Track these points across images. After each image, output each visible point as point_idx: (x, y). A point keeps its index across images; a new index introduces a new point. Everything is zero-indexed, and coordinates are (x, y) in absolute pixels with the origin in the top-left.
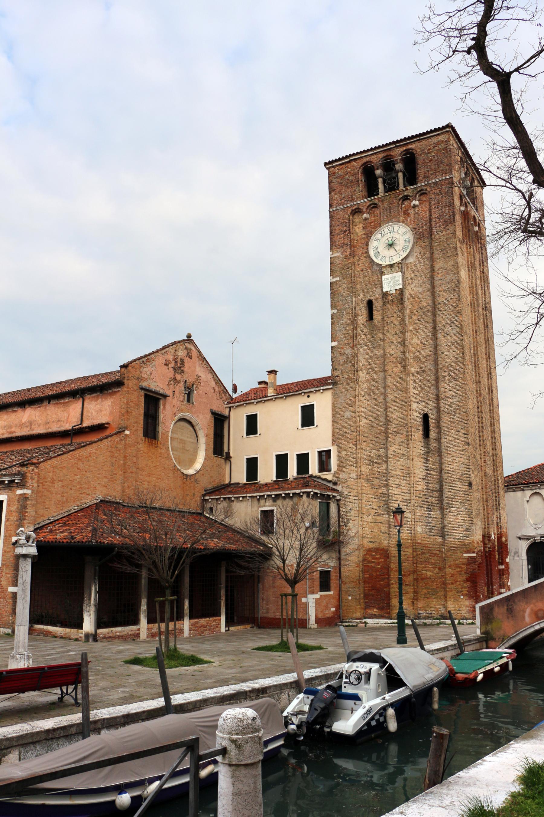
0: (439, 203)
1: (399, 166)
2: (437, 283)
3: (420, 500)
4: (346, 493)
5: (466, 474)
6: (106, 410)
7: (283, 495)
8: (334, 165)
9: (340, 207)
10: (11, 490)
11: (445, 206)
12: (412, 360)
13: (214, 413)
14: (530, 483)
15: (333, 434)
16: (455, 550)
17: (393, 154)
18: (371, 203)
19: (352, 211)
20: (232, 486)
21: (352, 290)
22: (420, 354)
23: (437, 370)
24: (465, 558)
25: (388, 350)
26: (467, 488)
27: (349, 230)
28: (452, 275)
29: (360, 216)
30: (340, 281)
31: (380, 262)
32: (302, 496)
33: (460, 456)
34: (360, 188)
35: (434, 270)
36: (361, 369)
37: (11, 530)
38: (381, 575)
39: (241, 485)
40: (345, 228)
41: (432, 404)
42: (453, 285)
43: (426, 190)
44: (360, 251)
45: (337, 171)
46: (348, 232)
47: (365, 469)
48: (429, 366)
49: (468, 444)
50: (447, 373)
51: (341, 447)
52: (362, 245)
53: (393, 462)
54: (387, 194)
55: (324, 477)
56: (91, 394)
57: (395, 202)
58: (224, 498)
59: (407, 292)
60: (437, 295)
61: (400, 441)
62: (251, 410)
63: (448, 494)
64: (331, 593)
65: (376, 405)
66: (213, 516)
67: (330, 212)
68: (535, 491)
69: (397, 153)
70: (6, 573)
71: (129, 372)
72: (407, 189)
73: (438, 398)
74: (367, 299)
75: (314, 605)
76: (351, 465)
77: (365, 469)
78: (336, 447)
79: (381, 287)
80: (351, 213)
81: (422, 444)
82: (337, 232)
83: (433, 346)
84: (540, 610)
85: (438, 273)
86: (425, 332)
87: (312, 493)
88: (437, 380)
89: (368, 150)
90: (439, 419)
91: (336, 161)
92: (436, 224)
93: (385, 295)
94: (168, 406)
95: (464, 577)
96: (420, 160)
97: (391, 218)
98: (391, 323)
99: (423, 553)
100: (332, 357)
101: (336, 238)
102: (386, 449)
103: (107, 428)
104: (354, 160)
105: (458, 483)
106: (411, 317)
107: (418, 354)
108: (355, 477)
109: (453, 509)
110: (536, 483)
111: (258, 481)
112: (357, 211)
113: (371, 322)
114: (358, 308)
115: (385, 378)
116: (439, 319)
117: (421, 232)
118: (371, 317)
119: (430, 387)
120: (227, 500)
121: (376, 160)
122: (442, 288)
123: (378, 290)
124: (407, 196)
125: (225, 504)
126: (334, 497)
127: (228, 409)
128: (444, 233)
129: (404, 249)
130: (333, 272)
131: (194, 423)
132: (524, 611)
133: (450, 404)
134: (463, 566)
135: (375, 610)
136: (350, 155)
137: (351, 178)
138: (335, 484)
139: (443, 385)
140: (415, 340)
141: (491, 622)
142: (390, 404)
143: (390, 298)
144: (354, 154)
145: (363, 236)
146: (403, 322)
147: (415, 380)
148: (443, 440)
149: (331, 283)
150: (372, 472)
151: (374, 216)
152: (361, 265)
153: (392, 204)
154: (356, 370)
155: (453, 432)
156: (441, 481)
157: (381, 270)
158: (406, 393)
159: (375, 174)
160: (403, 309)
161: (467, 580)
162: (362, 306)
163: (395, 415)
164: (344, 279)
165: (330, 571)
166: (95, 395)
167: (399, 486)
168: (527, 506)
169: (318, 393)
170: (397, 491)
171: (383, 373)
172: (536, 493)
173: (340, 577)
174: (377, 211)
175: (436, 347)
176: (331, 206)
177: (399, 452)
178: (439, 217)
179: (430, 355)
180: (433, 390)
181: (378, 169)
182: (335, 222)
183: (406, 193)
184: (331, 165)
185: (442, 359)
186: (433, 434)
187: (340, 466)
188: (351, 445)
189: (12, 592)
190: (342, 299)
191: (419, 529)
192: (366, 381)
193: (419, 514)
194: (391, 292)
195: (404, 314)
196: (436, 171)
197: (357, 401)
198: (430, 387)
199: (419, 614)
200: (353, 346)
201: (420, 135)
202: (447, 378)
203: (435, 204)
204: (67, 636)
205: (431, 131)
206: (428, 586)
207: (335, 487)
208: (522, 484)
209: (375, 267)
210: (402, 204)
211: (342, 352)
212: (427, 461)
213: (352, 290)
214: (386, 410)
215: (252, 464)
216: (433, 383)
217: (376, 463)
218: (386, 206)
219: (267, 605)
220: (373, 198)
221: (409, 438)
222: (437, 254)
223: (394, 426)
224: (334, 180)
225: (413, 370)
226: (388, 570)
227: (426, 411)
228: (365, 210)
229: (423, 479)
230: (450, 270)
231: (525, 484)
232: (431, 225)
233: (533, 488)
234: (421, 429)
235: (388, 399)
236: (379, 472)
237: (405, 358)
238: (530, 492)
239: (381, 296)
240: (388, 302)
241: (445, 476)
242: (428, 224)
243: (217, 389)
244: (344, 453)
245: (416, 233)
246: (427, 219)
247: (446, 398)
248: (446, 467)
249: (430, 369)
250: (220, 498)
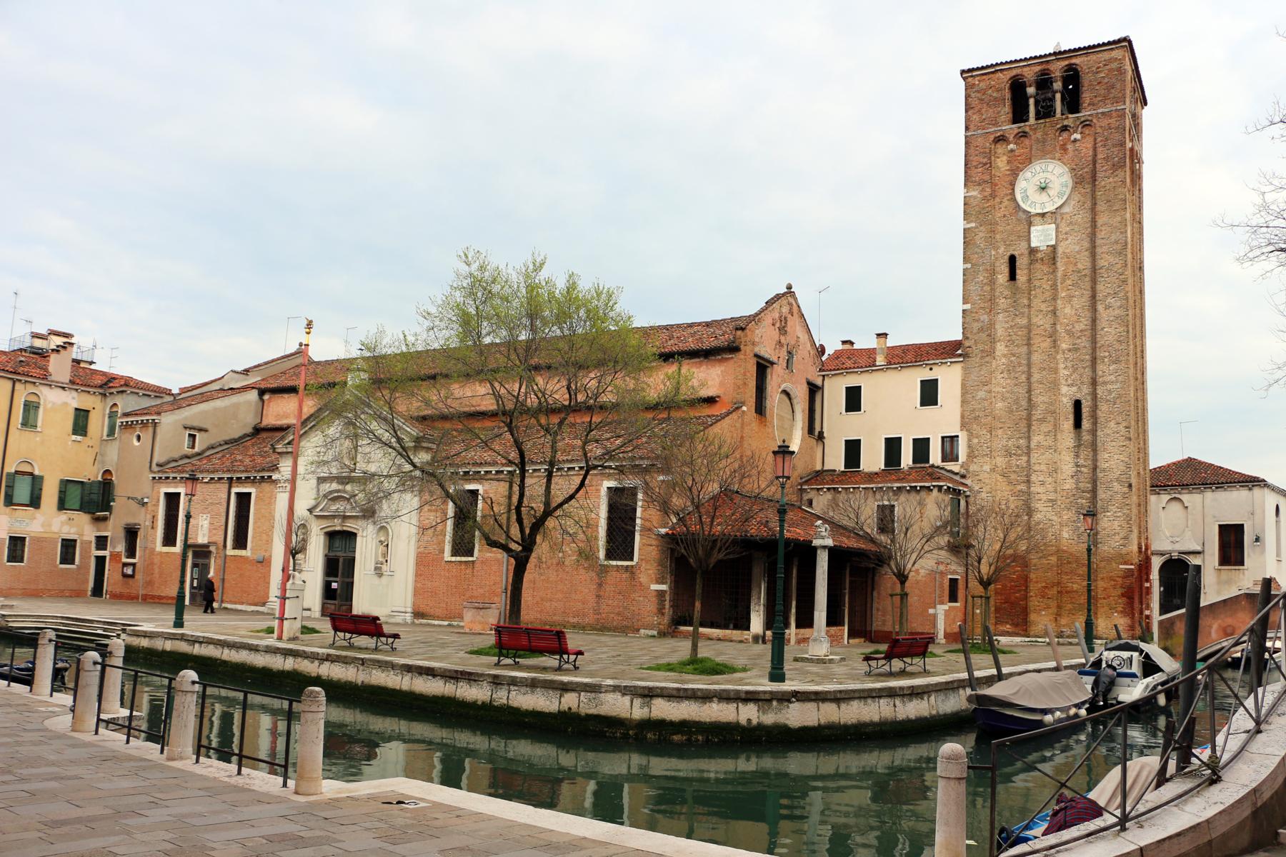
0: (1107, 140)
1: (1058, 85)
2: (1099, 242)
3: (1068, 501)
4: (977, 488)
5: (1126, 474)
6: (713, 379)
7: (908, 488)
8: (974, 74)
9: (979, 132)
11: (1114, 146)
12: (1063, 334)
13: (809, 383)
14: (1168, 486)
15: (963, 417)
16: (1109, 560)
17: (1052, 69)
18: (1020, 130)
19: (995, 138)
20: (825, 474)
21: (991, 241)
22: (1074, 327)
23: (1094, 349)
24: (1121, 570)
25: (1034, 320)
26: (1126, 490)
27: (991, 163)
28: (1118, 234)
29: (1004, 146)
30: (976, 227)
31: (1028, 209)
32: (932, 490)
33: (1119, 452)
34: (1006, 110)
35: (1095, 226)
36: (999, 341)
38: (1016, 586)
39: (837, 472)
40: (985, 160)
41: (1086, 389)
42: (1119, 247)
43: (1091, 121)
44: (1003, 191)
45: (977, 83)
46: (989, 165)
47: (1000, 461)
48: (1084, 342)
49: (1130, 439)
50: (1107, 354)
51: (972, 433)
52: (1005, 184)
53: (1036, 455)
54: (1042, 121)
55: (948, 468)
56: (690, 359)
57: (1051, 132)
58: (828, 489)
59: (1060, 250)
60: (1098, 257)
61: (1046, 430)
62: (852, 381)
63: (1103, 496)
64: (958, 604)
65: (1016, 385)
66: (813, 509)
67: (966, 137)
68: (1174, 496)
69: (1057, 68)
71: (746, 336)
72: (1067, 118)
73: (1094, 383)
74: (1009, 254)
75: (943, 617)
76: (985, 455)
77: (1000, 461)
78: (965, 433)
79: (1029, 241)
80: (993, 141)
81: (1072, 435)
82: (974, 164)
83: (1090, 319)
84: (1229, 626)
85: (1101, 230)
86: (1081, 300)
87: (945, 487)
88: (1094, 361)
89: (1021, 60)
90: (1095, 408)
91: (978, 69)
92: (1102, 167)
93: (1033, 251)
94: (774, 377)
95: (1120, 591)
96: (1086, 80)
97: (1045, 154)
98: (1040, 287)
99: (1069, 563)
100: (964, 323)
101: (973, 172)
102: (1029, 439)
103: (717, 401)
104: (1001, 70)
105: (1115, 484)
106: (1063, 281)
107: (1071, 327)
108: (988, 470)
109: (1109, 514)
110: (1176, 485)
111: (861, 469)
112: (1001, 139)
113: (1013, 282)
114: (997, 264)
115: (1029, 353)
116: (1100, 287)
117: (1081, 175)
118: (1013, 276)
119: (1084, 368)
120: (832, 491)
121: (1030, 74)
122: (1105, 249)
123: (1024, 245)
124: (1066, 126)
125: (829, 496)
126: (964, 492)
127: (821, 378)
128: (1111, 180)
129: (1060, 195)
130: (967, 215)
131: (792, 396)
132: (1210, 627)
133: (1110, 392)
134: (1118, 579)
135: (1008, 626)
136: (997, 64)
137: (995, 95)
138: (963, 477)
139: (1101, 367)
140: (1068, 310)
141: (1172, 638)
142: (1035, 385)
143: (1039, 255)
145: (1008, 173)
146: (1054, 287)
147: (1066, 359)
148: (1099, 433)
149: (964, 230)
150: (1009, 465)
151: (1023, 148)
152: (1004, 207)
153: (1047, 135)
154: (993, 340)
155: (1112, 424)
156: (1094, 482)
157: (1029, 220)
158: (1056, 373)
159: (1026, 92)
160: (1054, 271)
161: (1123, 595)
162: (1002, 261)
163: (1040, 399)
164: (981, 226)
165: (957, 579)
166: (697, 360)
167: (1043, 483)
168: (1162, 514)
169: (944, 366)
170: (1041, 490)
171: (1026, 347)
172: (1175, 498)
173: (967, 587)
174: (1027, 142)
175: (1094, 321)
176: (967, 128)
177: (1045, 443)
178: (1106, 159)
179: (1085, 330)
180: (1088, 372)
181: (1030, 86)
182: (972, 151)
183: (1066, 123)
185: (1102, 337)
186: (1086, 424)
187: (971, 456)
188: (984, 432)
190: (979, 251)
191: (1065, 535)
192: (1005, 356)
193: (1065, 517)
194: (1041, 249)
195: (1056, 276)
196: (1105, 98)
197: (993, 379)
198: (1084, 368)
199: (1062, 632)
200: (991, 311)
201: (1090, 47)
202: (1106, 360)
203: (1102, 141)
204: (727, 638)
205: (1104, 44)
206: (1073, 600)
207: (963, 481)
208: (1157, 486)
209: (1021, 214)
210: (1060, 136)
211: (976, 318)
212: (1077, 456)
213: (991, 241)
214: (1029, 391)
215: (853, 449)
216: (1089, 363)
217: (1014, 454)
218: (1039, 137)
219: (883, 616)
220: (1023, 124)
221: (1056, 427)
222: (1101, 206)
223: (1039, 412)
224: (973, 95)
225: (1064, 346)
226: (1026, 581)
227: (1078, 396)
228: (1011, 139)
229: (1072, 476)
230: (1116, 227)
231: (1161, 486)
232: (1095, 167)
233: (1172, 492)
234: (1071, 417)
235: (1033, 379)
236: (1018, 466)
237: (1055, 331)
238: (1167, 497)
239: (1026, 252)
240: (1037, 260)
241: (1100, 475)
242: (1091, 166)
243: (812, 352)
244: (976, 441)
245: (1075, 175)
246: (1090, 158)
247: (1105, 383)
248: (1102, 465)
249: (1085, 347)
250: (823, 488)
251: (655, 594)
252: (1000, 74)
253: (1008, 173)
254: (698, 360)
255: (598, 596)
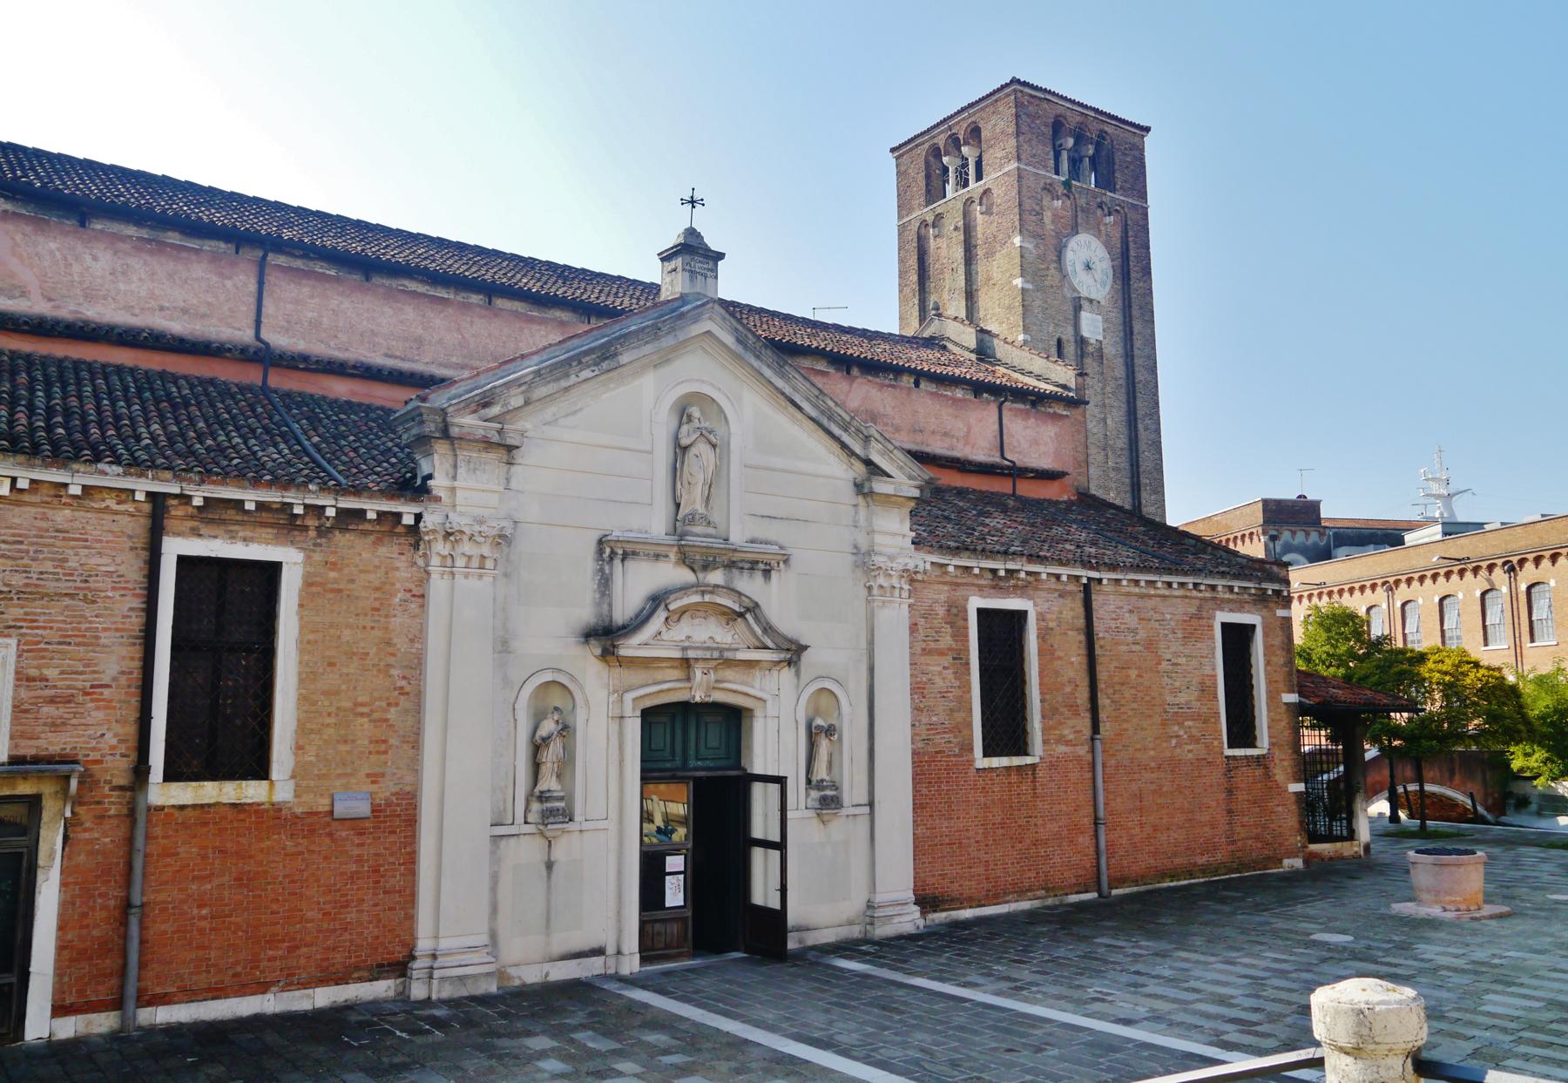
10: (1266, 607)
37: (1276, 681)
70: (1282, 760)
121: (1073, 120)
144: (1054, 94)
184: (1021, 88)
189: (1295, 793)
251: (1293, 798)
252: (1045, 105)
253: (1053, 234)
254: (1021, 406)
255: (1230, 812)
